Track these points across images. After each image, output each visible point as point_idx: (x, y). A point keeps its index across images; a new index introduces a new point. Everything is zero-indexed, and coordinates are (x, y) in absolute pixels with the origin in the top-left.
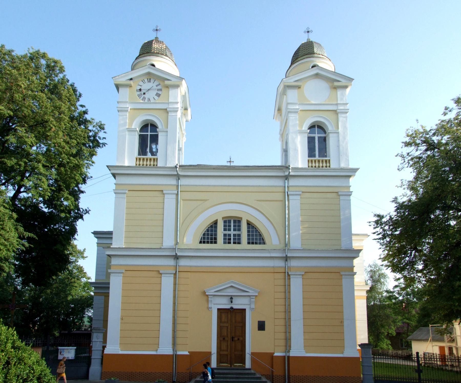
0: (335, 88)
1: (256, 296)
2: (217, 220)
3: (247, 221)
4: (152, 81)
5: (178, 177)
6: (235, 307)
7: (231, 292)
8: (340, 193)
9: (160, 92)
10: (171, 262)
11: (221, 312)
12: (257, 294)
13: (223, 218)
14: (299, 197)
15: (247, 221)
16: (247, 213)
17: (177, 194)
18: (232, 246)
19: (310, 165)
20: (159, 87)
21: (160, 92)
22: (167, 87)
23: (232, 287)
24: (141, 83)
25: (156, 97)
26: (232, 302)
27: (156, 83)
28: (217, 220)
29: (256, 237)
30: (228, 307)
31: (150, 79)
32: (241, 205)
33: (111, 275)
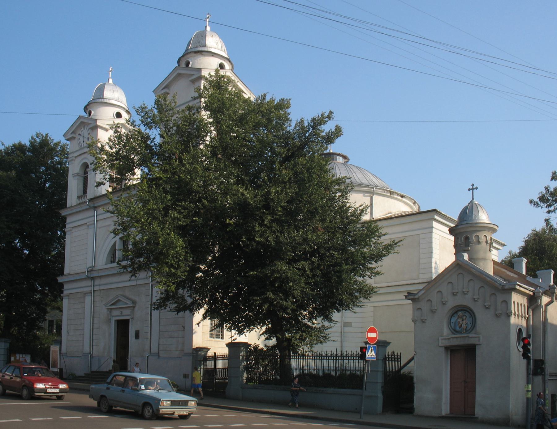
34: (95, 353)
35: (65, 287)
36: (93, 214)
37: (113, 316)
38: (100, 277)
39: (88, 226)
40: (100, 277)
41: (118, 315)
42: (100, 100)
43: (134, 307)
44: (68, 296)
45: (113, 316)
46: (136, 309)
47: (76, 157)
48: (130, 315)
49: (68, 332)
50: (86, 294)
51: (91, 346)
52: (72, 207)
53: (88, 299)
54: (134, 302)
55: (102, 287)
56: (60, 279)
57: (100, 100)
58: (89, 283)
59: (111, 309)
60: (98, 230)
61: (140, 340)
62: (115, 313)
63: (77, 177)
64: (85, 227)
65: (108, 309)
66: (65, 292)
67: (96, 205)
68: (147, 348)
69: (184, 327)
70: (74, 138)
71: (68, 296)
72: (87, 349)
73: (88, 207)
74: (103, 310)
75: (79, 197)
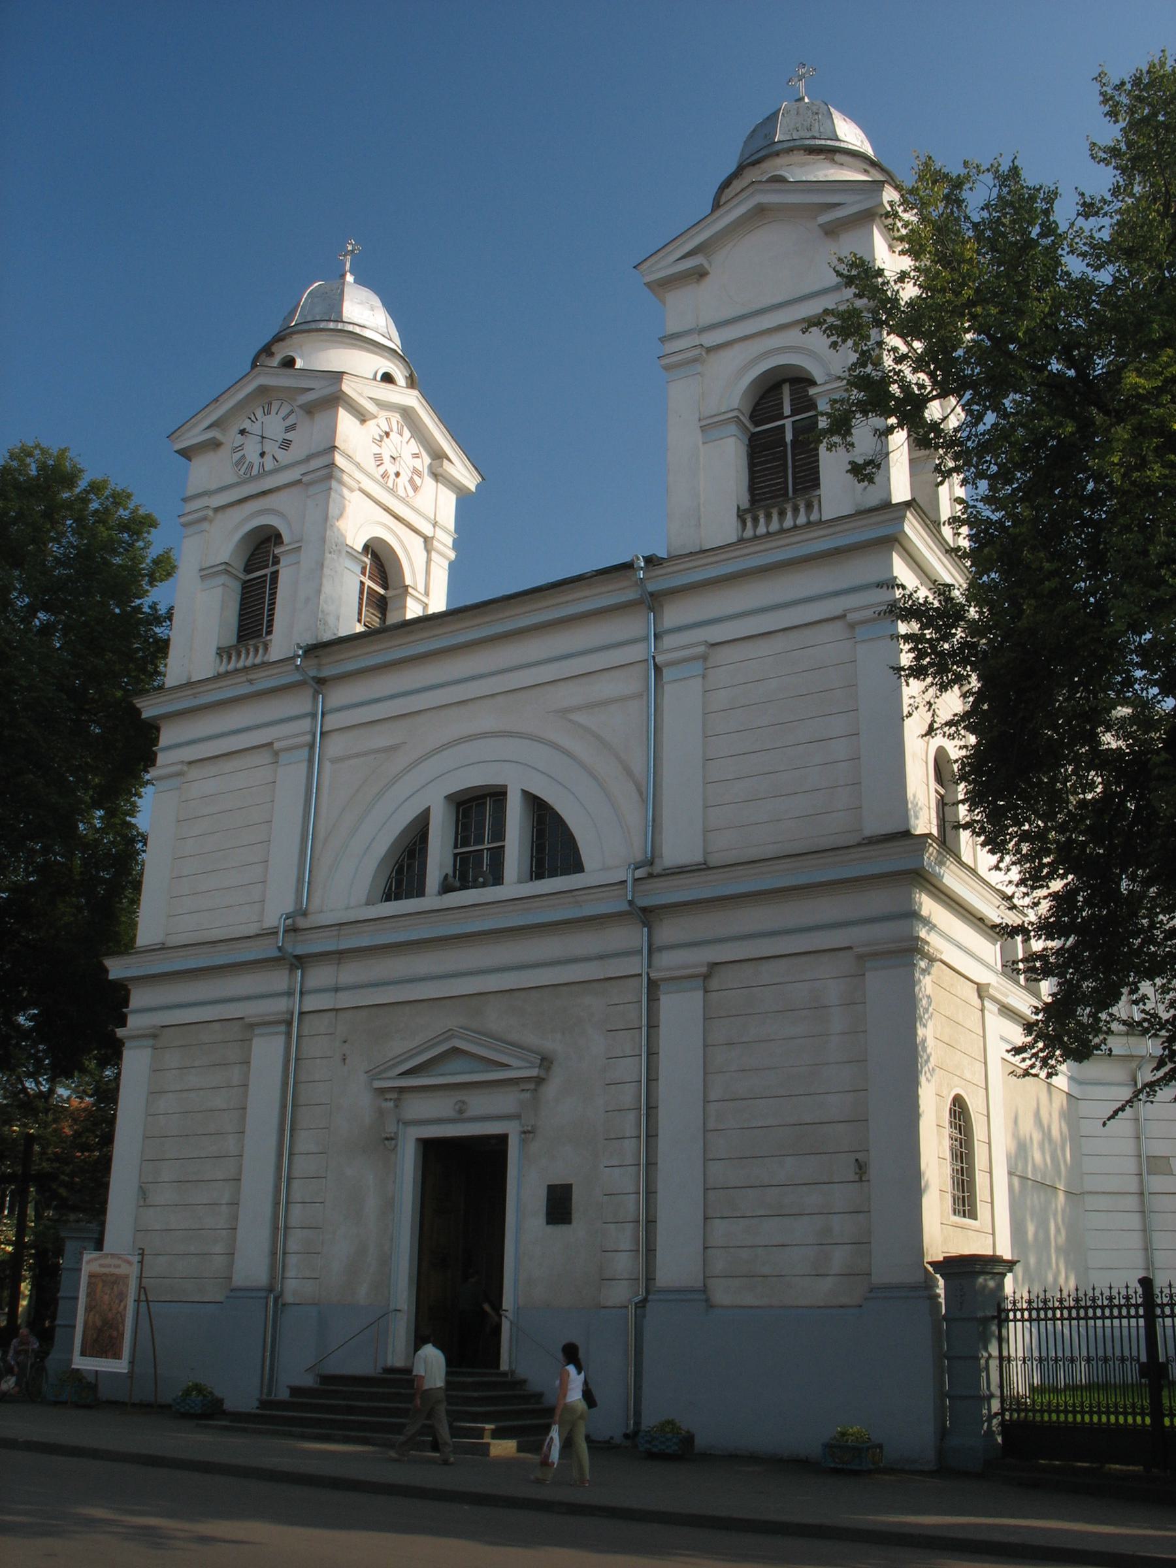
2: (427, 811)
3: (526, 794)
8: (851, 617)
9: (289, 436)
12: (534, 1072)
13: (449, 798)
14: (697, 668)
15: (526, 794)
17: (312, 746)
20: (289, 422)
21: (289, 436)
22: (310, 410)
23: (455, 1051)
25: (281, 455)
27: (285, 410)
29: (554, 847)
34: (294, 1287)
35: (138, 998)
36: (307, 707)
37: (407, 1123)
38: (340, 956)
39: (276, 754)
40: (340, 956)
42: (332, 325)
43: (539, 1081)
44: (153, 1035)
45: (407, 1123)
46: (550, 1090)
47: (217, 510)
48: (517, 1117)
49: (143, 1192)
50: (250, 1027)
51: (277, 1258)
52: (189, 684)
53: (267, 1052)
54: (546, 1062)
55: (345, 1000)
56: (117, 968)
57: (332, 325)
58: (279, 980)
59: (402, 1090)
60: (327, 765)
61: (578, 1228)
62: (417, 1107)
64: (264, 757)
65: (382, 1091)
66: (135, 1022)
67: (325, 673)
68: (624, 1263)
69: (861, 1167)
71: (155, 1036)
72: (252, 1268)
73: (297, 677)
74: (346, 1094)
75: (223, 652)
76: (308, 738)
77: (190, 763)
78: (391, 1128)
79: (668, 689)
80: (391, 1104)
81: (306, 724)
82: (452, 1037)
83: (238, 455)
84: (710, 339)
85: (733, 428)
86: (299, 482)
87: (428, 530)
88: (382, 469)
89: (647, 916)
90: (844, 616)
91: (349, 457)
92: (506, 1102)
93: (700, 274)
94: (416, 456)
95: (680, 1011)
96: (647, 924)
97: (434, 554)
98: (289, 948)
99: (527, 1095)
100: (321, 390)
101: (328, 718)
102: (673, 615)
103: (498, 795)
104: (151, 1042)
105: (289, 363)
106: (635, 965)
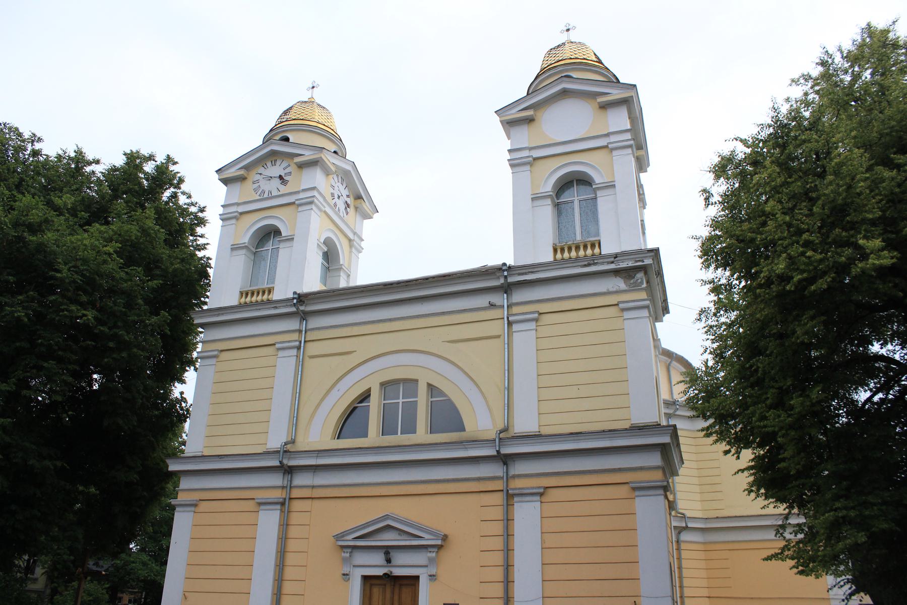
0: (604, 107)
1: (440, 547)
2: (369, 390)
4: (278, 163)
5: (304, 316)
6: (397, 572)
7: (389, 539)
10: (277, 480)
11: (371, 585)
12: (439, 542)
14: (532, 325)
16: (426, 370)
18: (400, 438)
19: (559, 256)
22: (301, 166)
23: (389, 527)
24: (261, 170)
25: (282, 188)
26: (389, 561)
27: (285, 164)
28: (369, 390)
29: (446, 416)
30: (379, 572)
31: (276, 161)
32: (415, 355)
33: (177, 509)
41: (374, 565)
47: (241, 214)
56: (174, 466)
59: (355, 548)
62: (361, 558)
63: (244, 251)
65: (343, 547)
66: (182, 497)
70: (241, 179)
73: (294, 309)
76: (297, 343)
77: (222, 351)
78: (346, 571)
79: (516, 337)
80: (348, 555)
81: (295, 336)
82: (385, 520)
83: (257, 185)
84: (537, 154)
85: (549, 201)
86: (293, 203)
87: (351, 236)
88: (334, 201)
89: (506, 460)
90: (617, 305)
91: (320, 194)
92: (420, 558)
93: (530, 120)
94: (348, 196)
95: (527, 514)
96: (505, 463)
97: (353, 250)
98: (285, 462)
99: (434, 554)
100: (308, 155)
101: (308, 333)
102: (518, 296)
103: (411, 384)
104: (193, 509)
105: (287, 139)
106: (499, 485)
